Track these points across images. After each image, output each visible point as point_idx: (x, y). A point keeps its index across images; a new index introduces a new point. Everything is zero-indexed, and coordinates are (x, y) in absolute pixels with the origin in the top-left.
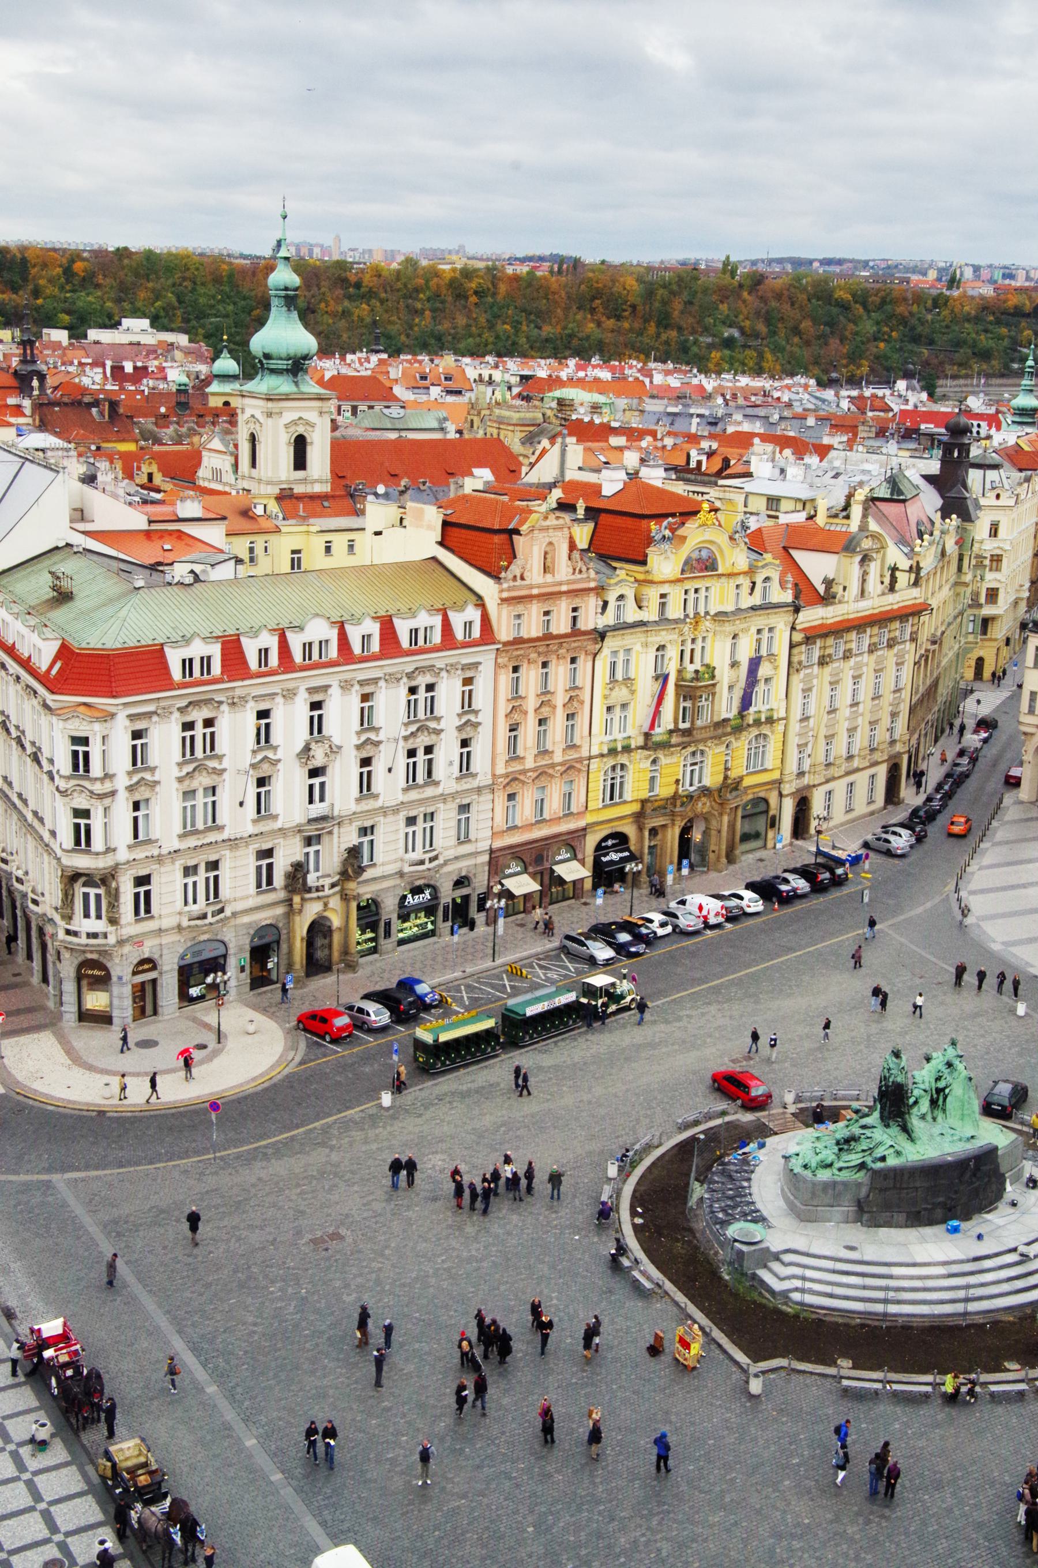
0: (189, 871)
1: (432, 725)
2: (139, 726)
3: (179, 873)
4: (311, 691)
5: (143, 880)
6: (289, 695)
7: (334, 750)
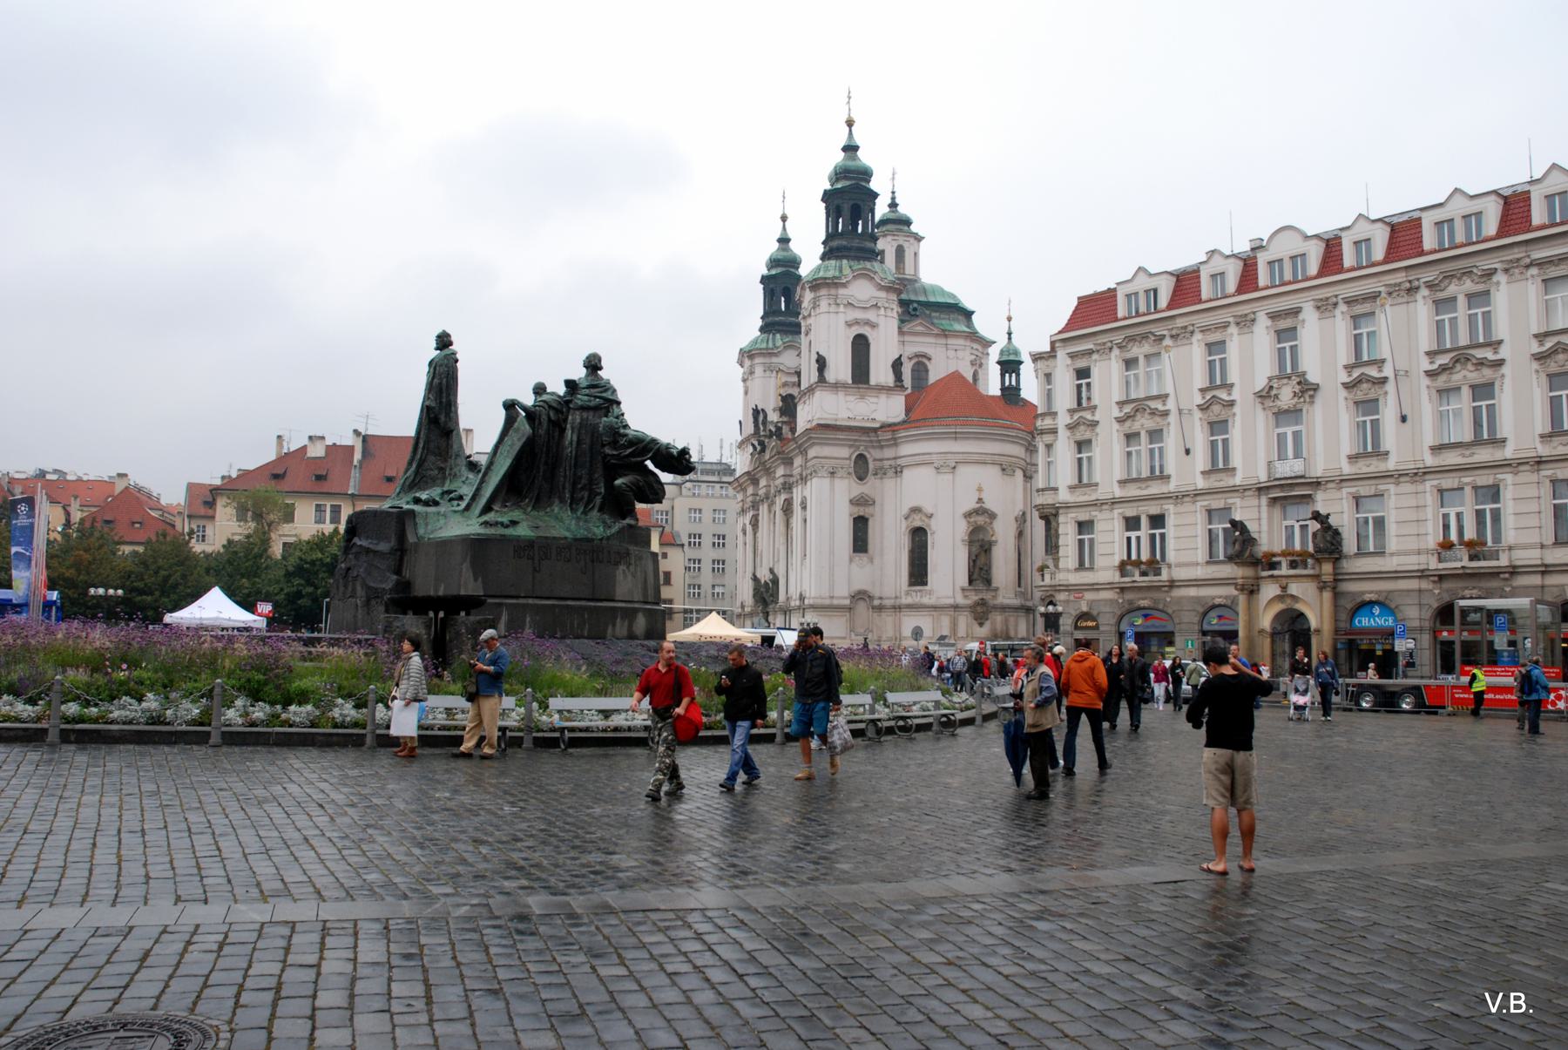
0: (1132, 523)
1: (1480, 354)
2: (1081, 364)
3: (1118, 525)
4: (1274, 316)
5: (1084, 526)
6: (1246, 322)
7: (1308, 390)
